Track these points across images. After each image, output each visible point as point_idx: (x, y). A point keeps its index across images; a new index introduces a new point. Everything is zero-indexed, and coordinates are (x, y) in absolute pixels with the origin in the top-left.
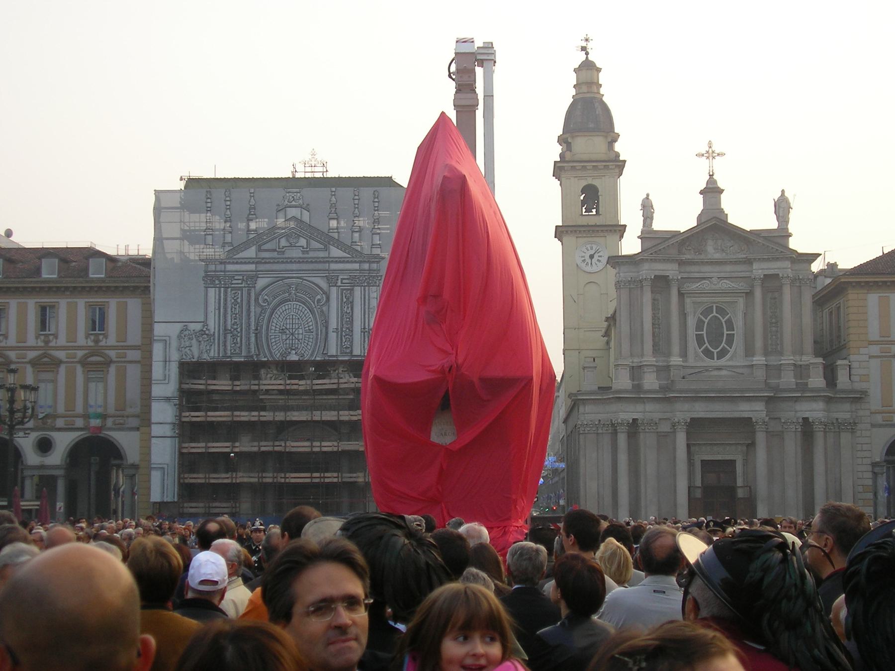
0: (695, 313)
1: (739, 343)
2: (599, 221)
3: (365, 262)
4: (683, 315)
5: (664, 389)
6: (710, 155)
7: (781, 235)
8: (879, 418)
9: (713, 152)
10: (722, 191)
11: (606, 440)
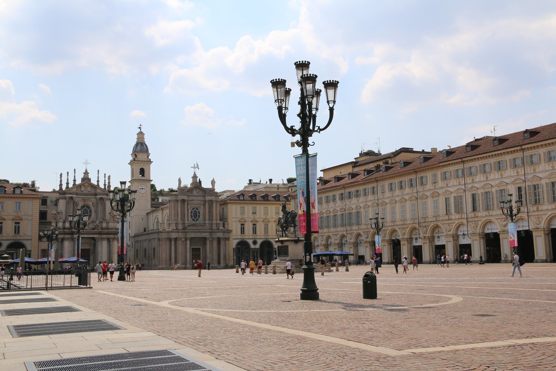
2: (143, 178)
4: (188, 210)
5: (183, 229)
8: (234, 237)
11: (168, 242)
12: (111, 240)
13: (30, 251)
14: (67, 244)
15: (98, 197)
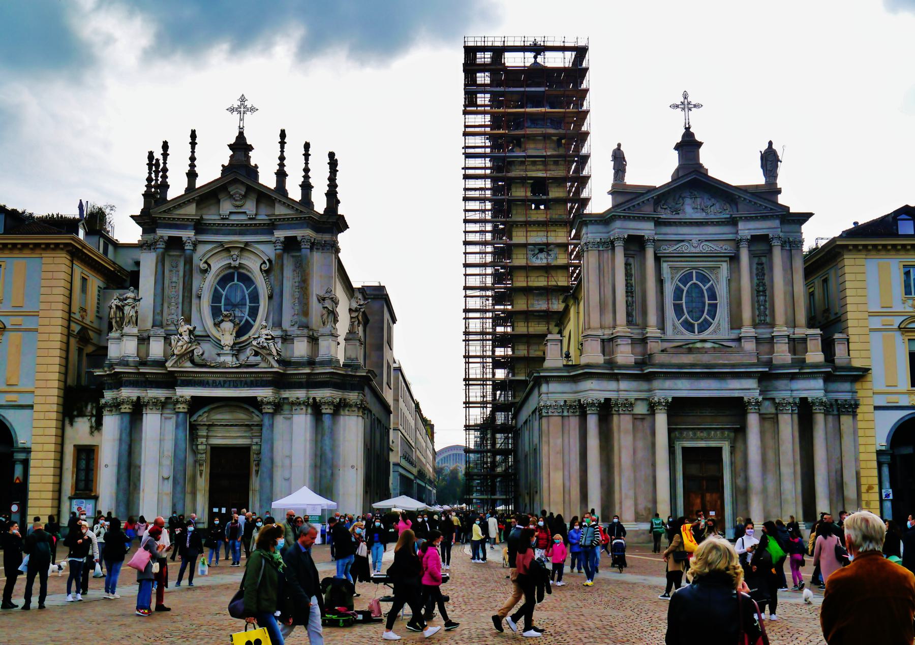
0: (672, 278)
1: (722, 313)
4: (660, 282)
5: (640, 364)
6: (686, 105)
7: (771, 191)
8: (881, 401)
9: (689, 103)
10: (700, 144)
11: (574, 422)
12: (326, 410)
13: (28, 451)
14: (151, 421)
15: (280, 234)
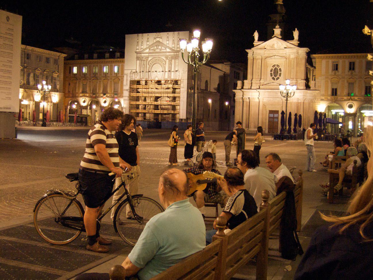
3: (175, 52)
